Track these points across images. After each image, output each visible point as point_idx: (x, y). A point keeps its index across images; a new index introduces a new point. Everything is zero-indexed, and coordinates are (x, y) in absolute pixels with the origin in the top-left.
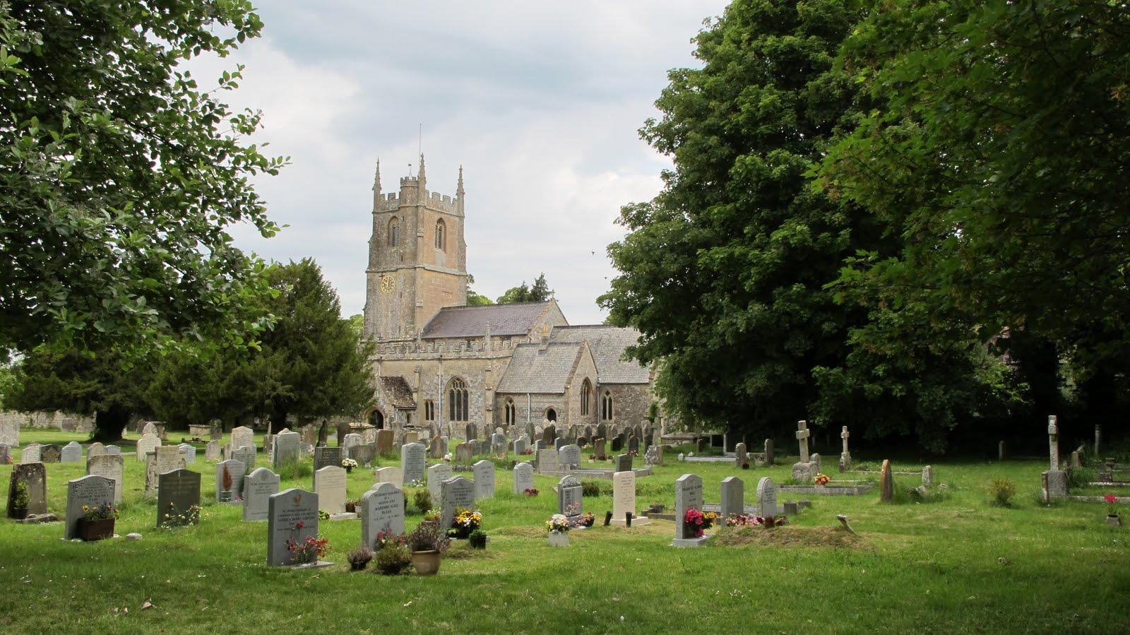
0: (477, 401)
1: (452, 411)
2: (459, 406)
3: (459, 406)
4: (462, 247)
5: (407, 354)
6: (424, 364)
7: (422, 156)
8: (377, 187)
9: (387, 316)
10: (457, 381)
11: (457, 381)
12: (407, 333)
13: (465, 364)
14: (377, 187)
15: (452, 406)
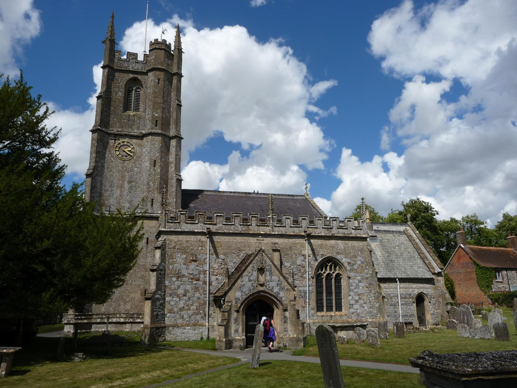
0: (357, 287)
2: (329, 293)
3: (329, 293)
9: (122, 187)
15: (319, 293)
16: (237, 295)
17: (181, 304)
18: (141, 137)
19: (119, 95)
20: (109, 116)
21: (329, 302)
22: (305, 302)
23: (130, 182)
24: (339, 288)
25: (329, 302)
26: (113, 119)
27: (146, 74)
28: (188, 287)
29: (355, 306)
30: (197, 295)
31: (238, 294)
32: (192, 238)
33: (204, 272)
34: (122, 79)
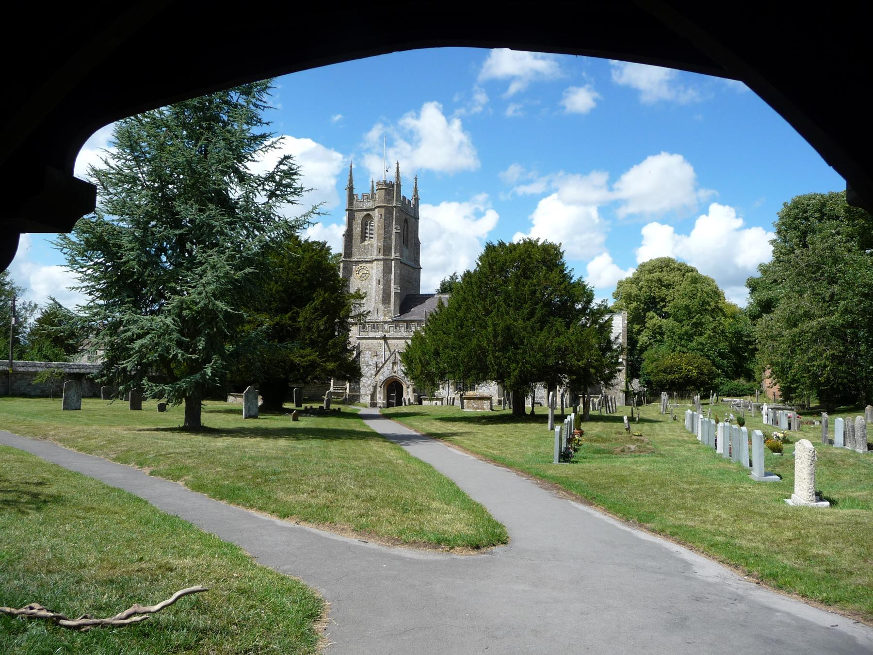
4: (417, 244)
8: (351, 189)
12: (385, 315)
14: (351, 189)
18: (371, 262)
19: (357, 230)
20: (351, 248)
26: (354, 250)
27: (374, 210)
32: (375, 341)
34: (359, 217)
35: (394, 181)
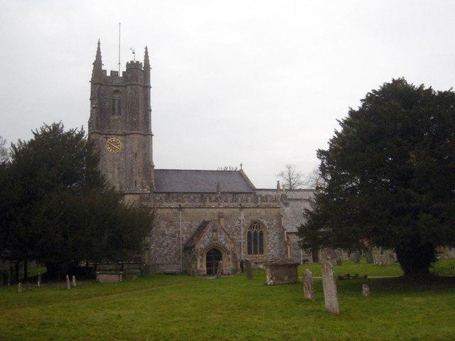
1: (249, 248)
5: (208, 203)
6: (226, 212)
7: (146, 48)
8: (98, 64)
9: (113, 172)
10: (256, 224)
11: (256, 224)
13: (263, 212)
14: (98, 64)
15: (249, 243)
16: (202, 245)
17: (165, 252)
21: (255, 248)
22: (241, 250)
23: (118, 169)
24: (262, 240)
25: (255, 248)
28: (169, 242)
29: (272, 251)
30: (174, 246)
31: (202, 246)
33: (179, 232)
35: (142, 60)
